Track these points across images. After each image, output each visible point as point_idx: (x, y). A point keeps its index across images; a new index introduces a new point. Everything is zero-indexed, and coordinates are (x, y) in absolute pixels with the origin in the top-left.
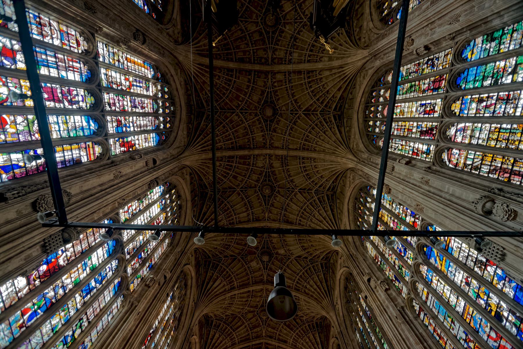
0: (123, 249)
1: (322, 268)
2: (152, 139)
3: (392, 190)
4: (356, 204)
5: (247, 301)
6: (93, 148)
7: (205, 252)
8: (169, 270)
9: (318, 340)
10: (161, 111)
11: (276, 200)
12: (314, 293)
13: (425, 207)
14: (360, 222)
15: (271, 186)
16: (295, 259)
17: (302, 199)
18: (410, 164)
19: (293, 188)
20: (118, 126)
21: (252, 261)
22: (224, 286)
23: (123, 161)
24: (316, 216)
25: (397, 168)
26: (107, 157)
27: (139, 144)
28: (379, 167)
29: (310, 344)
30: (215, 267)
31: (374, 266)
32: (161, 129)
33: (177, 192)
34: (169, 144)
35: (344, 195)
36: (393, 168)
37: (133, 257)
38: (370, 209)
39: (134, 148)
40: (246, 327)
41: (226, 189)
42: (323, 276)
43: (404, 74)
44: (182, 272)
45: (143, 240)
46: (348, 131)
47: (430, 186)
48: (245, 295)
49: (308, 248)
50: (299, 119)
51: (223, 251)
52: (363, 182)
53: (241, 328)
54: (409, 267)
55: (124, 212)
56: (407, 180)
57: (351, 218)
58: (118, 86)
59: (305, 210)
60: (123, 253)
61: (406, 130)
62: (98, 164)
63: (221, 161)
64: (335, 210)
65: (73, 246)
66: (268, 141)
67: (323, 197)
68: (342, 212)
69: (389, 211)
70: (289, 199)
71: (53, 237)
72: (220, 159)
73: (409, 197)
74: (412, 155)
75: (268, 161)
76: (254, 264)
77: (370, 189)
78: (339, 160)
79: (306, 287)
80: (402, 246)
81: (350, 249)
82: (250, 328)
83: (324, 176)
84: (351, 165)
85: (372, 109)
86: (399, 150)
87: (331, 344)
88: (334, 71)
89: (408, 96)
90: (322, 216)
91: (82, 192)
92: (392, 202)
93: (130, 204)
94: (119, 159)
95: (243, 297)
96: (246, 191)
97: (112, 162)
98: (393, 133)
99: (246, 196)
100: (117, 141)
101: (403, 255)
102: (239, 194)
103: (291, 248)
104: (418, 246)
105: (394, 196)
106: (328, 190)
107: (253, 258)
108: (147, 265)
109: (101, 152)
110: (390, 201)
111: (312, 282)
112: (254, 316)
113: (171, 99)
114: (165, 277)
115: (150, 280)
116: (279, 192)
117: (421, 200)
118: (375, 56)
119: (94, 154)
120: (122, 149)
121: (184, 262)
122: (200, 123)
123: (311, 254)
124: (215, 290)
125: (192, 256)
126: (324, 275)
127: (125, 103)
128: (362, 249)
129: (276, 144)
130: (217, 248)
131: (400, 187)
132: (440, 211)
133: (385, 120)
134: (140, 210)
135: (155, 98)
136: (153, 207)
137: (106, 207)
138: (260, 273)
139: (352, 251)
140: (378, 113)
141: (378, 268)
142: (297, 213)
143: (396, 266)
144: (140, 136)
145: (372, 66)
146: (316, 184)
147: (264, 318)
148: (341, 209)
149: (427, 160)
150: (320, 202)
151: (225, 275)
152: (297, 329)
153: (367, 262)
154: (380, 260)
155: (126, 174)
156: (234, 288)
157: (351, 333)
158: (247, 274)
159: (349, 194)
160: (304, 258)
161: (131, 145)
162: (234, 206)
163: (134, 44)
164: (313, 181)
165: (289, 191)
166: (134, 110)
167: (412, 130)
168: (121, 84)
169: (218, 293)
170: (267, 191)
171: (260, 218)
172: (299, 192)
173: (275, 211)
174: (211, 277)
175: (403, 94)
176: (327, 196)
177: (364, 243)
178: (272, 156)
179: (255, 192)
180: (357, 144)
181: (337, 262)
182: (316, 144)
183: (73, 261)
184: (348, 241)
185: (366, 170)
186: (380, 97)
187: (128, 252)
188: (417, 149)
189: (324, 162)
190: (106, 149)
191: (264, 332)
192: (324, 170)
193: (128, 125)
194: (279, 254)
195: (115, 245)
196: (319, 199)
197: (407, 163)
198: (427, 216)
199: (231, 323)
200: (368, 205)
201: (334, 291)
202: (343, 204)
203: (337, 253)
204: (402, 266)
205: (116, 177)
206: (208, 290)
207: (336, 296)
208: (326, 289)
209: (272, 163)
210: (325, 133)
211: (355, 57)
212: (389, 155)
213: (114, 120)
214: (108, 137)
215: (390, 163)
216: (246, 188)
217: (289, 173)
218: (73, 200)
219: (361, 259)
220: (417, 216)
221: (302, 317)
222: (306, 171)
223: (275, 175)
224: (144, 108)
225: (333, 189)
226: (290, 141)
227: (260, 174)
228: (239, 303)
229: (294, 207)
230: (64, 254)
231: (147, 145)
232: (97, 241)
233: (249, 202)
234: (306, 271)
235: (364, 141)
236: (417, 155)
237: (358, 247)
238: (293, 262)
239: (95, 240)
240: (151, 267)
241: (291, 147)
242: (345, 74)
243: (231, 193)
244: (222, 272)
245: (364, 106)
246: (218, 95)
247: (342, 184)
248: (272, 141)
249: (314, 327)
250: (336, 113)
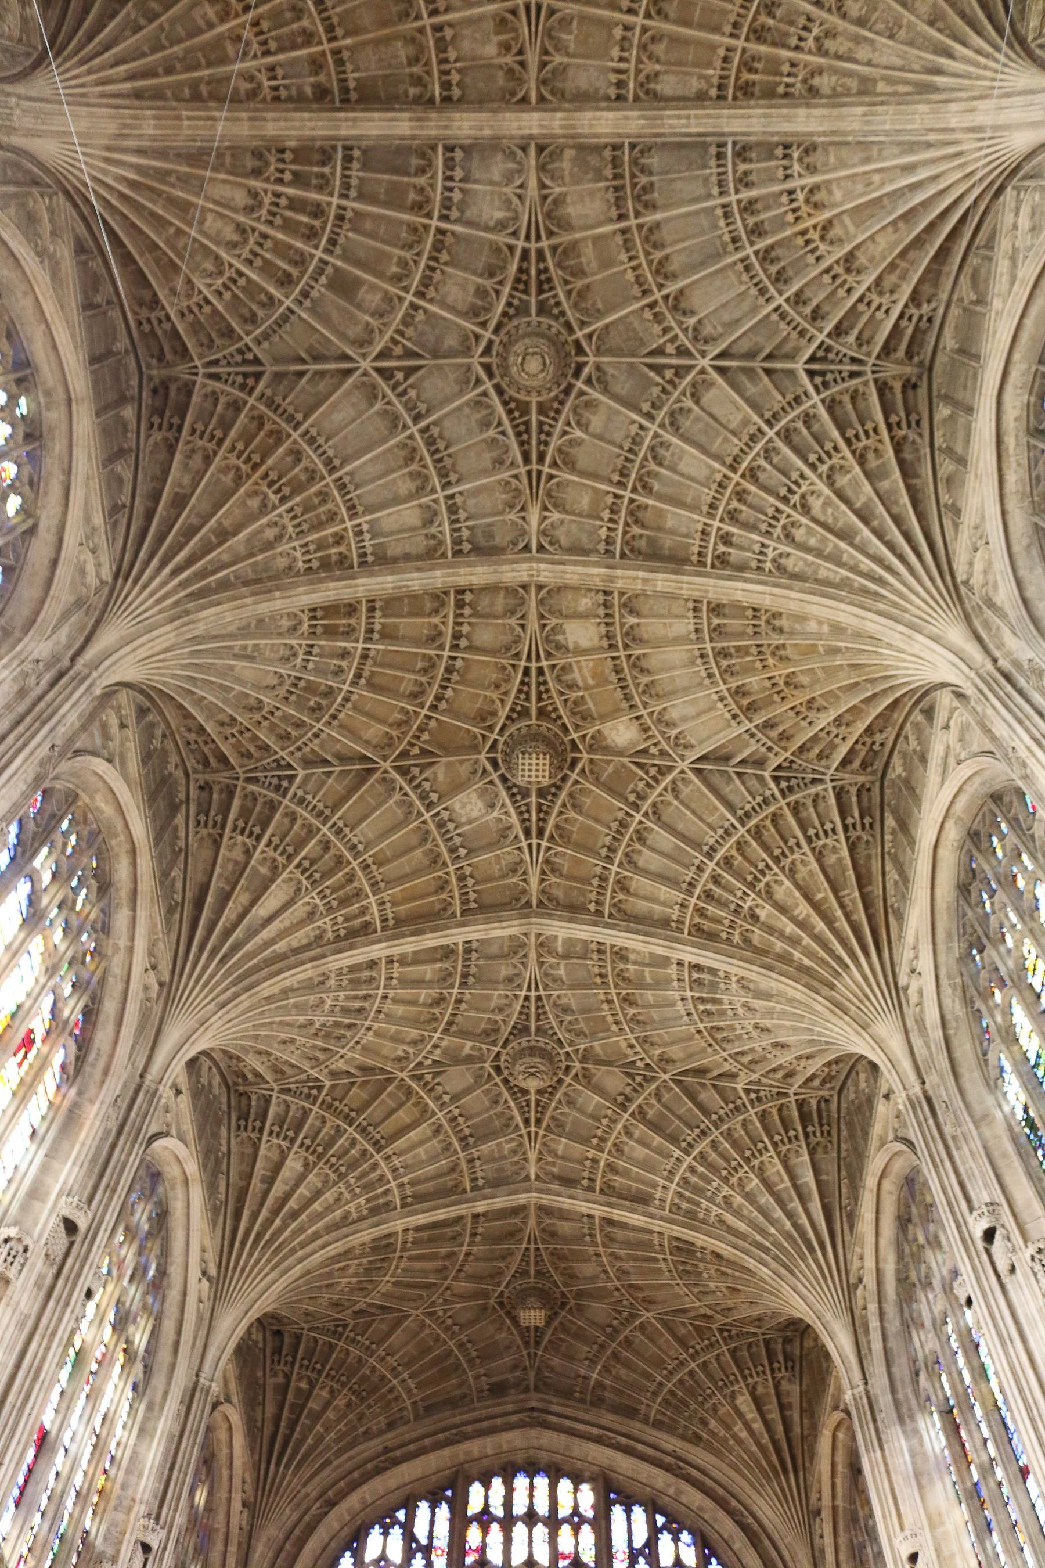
5: (440, 1000)
7: (201, 730)
9: (808, 1178)
12: (794, 941)
19: (682, 352)
21: (458, 787)
22: (311, 915)
24: (816, 504)
29: (766, 1199)
35: (977, 357)
40: (437, 1131)
42: (845, 852)
48: (428, 971)
49: (769, 702)
53: (413, 1135)
57: (1012, 479)
68: (962, 461)
70: (661, 415)
75: (533, 183)
79: (755, 917)
82: (463, 1139)
83: (862, 259)
87: (870, 1182)
95: (419, 983)
96: (409, 371)
102: (372, 394)
107: (464, 770)
111: (785, 889)
112: (479, 1079)
124: (265, 934)
126: (852, 848)
138: (506, 854)
147: (532, 1085)
148: (959, 449)
152: (703, 1133)
156: (366, 928)
157: (971, 1077)
158: (435, 859)
164: (798, 299)
165: (658, 369)
169: (280, 947)
176: (883, 388)
178: (557, 154)
181: (923, 759)
184: (990, 604)
189: (868, 160)
191: (533, 1156)
196: (832, 405)
199: (359, 1111)
201: (900, 917)
202: (970, 410)
207: (909, 939)
208: (861, 916)
209: (559, 201)
217: (658, 255)
221: (732, 1076)
222: (757, 231)
223: (579, 272)
228: (400, 1010)
233: (430, 442)
234: (757, 833)
238: (685, 791)
249: (786, 1125)
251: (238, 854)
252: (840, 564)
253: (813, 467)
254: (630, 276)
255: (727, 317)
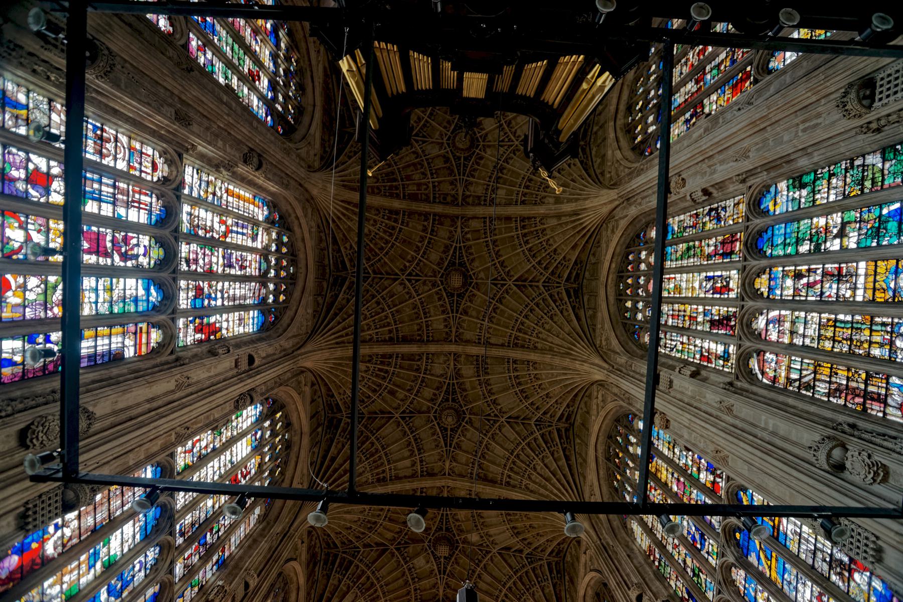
0: (172, 526)
1: (551, 572)
2: (251, 321)
3: (672, 422)
4: (609, 448)
6: (148, 333)
7: (329, 535)
8: (256, 570)
10: (272, 273)
11: (464, 436)
13: (731, 455)
14: (618, 481)
15: (456, 411)
16: (500, 554)
17: (512, 435)
18: (699, 377)
19: (496, 416)
20: (196, 297)
21: (417, 555)
23: (195, 356)
24: (538, 468)
25: (677, 383)
26: (169, 351)
27: (227, 329)
28: (645, 380)
30: (346, 566)
31: (648, 569)
32: (269, 304)
33: (286, 417)
34: (280, 331)
35: (588, 430)
36: (671, 382)
37: (189, 542)
38: (633, 457)
39: (218, 335)
41: (376, 413)
42: (552, 588)
43: (676, 229)
44: (280, 574)
45: (213, 507)
46: (590, 317)
47: (736, 417)
49: (524, 532)
50: (508, 293)
51: (363, 533)
52: (621, 407)
54: (712, 571)
55: (185, 452)
56: (695, 404)
57: (601, 472)
58: (207, 232)
59: (518, 456)
60: (172, 533)
61: (687, 318)
62: (153, 362)
63: (369, 361)
64: (573, 458)
65: (79, 517)
66: (454, 330)
67: (550, 432)
68: (585, 461)
69: (670, 462)
70: (489, 435)
71: (44, 498)
72: (367, 358)
73: (702, 436)
74: (700, 360)
75: (452, 364)
76: (420, 562)
77: (633, 419)
78: (578, 366)
80: (697, 529)
81: (602, 534)
83: (551, 395)
84: (598, 376)
85: (630, 281)
86: (678, 351)
88: (564, 220)
89: (685, 262)
90: (547, 467)
91: (115, 413)
92: (673, 445)
93: (198, 438)
94: (190, 354)
96: (410, 418)
97: (177, 359)
98: (666, 322)
99: (410, 429)
100: (191, 322)
101: (699, 546)
102: (399, 424)
103: (492, 531)
104: (724, 530)
105: (676, 434)
106: (560, 419)
107: (419, 549)
108: (215, 558)
109: (159, 340)
110: (669, 443)
113: (292, 255)
114: (247, 585)
115: (216, 590)
116: (470, 422)
117: (722, 442)
118: (628, 200)
119: (148, 343)
120: (198, 336)
121: (285, 555)
122: (337, 296)
123: (530, 544)
125: (303, 542)
126: (554, 586)
127: (214, 259)
128: (625, 535)
129: (468, 335)
130: (351, 528)
131: (685, 418)
132: (757, 462)
133: (650, 299)
134: (214, 449)
135: (264, 253)
136: (239, 444)
137: (154, 442)
138: (432, 580)
139: (605, 539)
140: (639, 288)
141: (654, 574)
142: (503, 461)
143: (689, 570)
144: (231, 315)
145: (625, 214)
146: (538, 408)
149: (726, 370)
150: (546, 443)
151: (363, 585)
153: (635, 561)
154: (657, 556)
155: (198, 382)
158: (406, 582)
159: (596, 428)
160: (515, 551)
161: (213, 330)
162: (388, 446)
163: (242, 169)
164: (532, 404)
165: (489, 420)
166: (227, 270)
167: (696, 317)
168: (212, 229)
170: (450, 419)
171: (436, 471)
172: (508, 422)
173: (463, 457)
174: (336, 588)
175: (677, 260)
176: (558, 430)
177: (628, 523)
178: (459, 356)
179: (429, 420)
180: (607, 339)
181: (578, 559)
182: (538, 337)
183: (73, 547)
185: (625, 385)
186: (640, 263)
187: (181, 530)
188: (708, 351)
189: (552, 369)
190: (170, 336)
192: (551, 384)
193: (213, 295)
194: (468, 543)
195: (158, 516)
196: (543, 436)
197: (694, 375)
198: (736, 472)
200: (631, 449)
203: (579, 542)
204: (700, 570)
205: (179, 387)
206: (336, 470)
210: (552, 318)
211: (597, 199)
212: (661, 360)
213: (191, 286)
214: (177, 316)
215: (664, 374)
216: (411, 412)
217: (489, 388)
218: (97, 426)
219: (622, 554)
220: (719, 472)
222: (519, 384)
224: (245, 268)
225: (568, 418)
226: (491, 331)
227: (438, 389)
229: (498, 450)
230: (59, 533)
231: (241, 330)
232: (125, 508)
233: (416, 440)
235: (618, 333)
236: (709, 361)
237: (617, 531)
238: (495, 560)
239: (123, 505)
240: (222, 564)
241: (493, 341)
242: (582, 224)
243: (383, 421)
244: (359, 577)
245: (615, 276)
246: (371, 250)
247: (585, 409)
248: (461, 330)
250: (569, 285)
251: (336, 582)
252: (547, 490)
253: (537, 456)
254: (481, 393)
255: (510, 407)
